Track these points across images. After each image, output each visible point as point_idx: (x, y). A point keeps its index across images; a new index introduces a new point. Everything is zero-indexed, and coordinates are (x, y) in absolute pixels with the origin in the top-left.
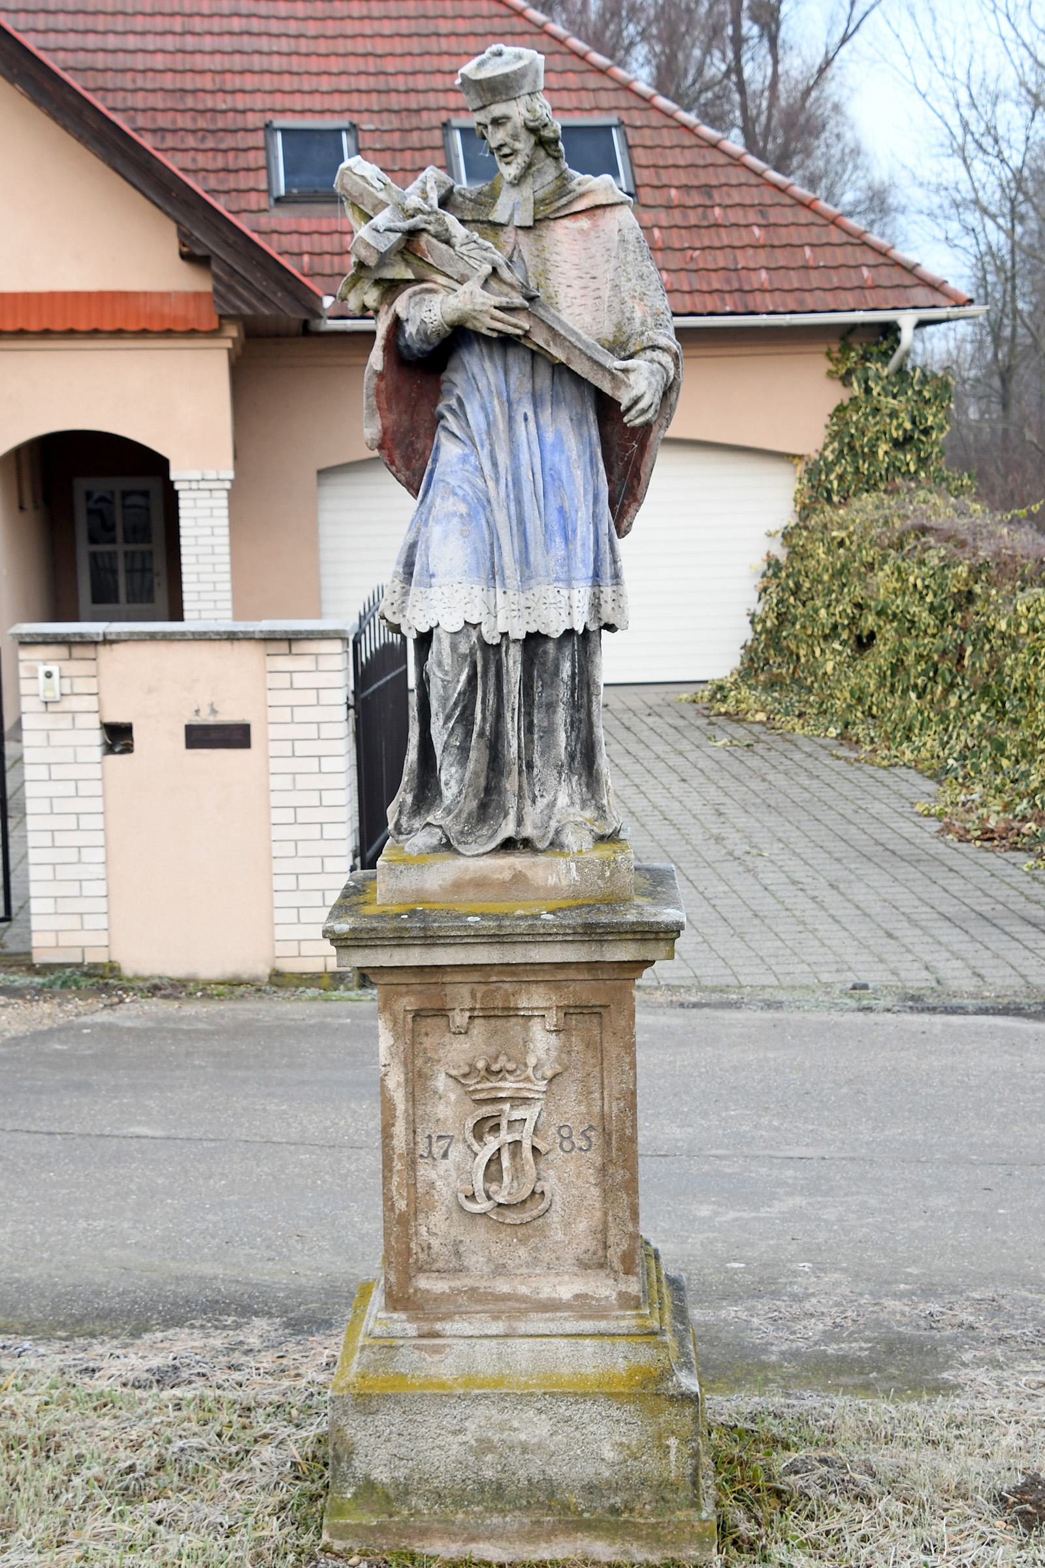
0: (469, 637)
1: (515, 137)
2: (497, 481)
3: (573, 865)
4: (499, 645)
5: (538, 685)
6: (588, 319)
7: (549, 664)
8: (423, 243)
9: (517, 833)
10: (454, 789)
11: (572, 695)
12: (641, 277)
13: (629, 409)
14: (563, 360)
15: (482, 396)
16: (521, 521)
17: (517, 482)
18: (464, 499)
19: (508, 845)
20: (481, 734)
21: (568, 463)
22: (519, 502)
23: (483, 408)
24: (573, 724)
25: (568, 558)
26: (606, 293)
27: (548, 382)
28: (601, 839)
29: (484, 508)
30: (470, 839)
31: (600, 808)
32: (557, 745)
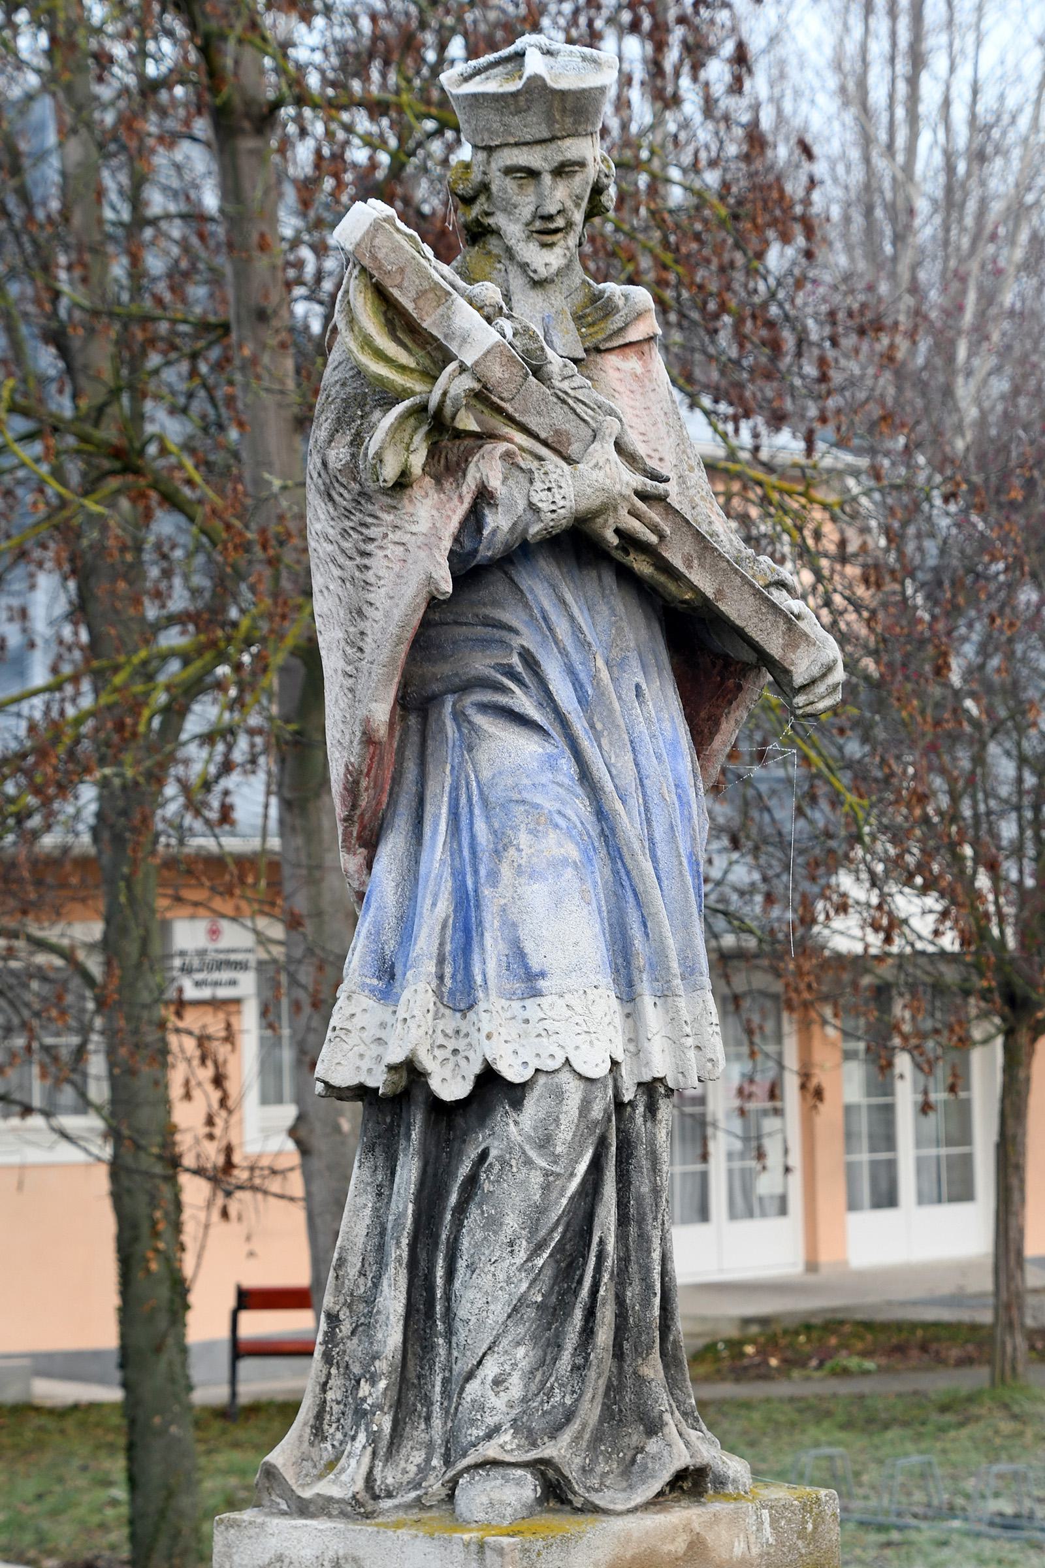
3: (765, 1513)
14: (709, 591)
15: (563, 652)
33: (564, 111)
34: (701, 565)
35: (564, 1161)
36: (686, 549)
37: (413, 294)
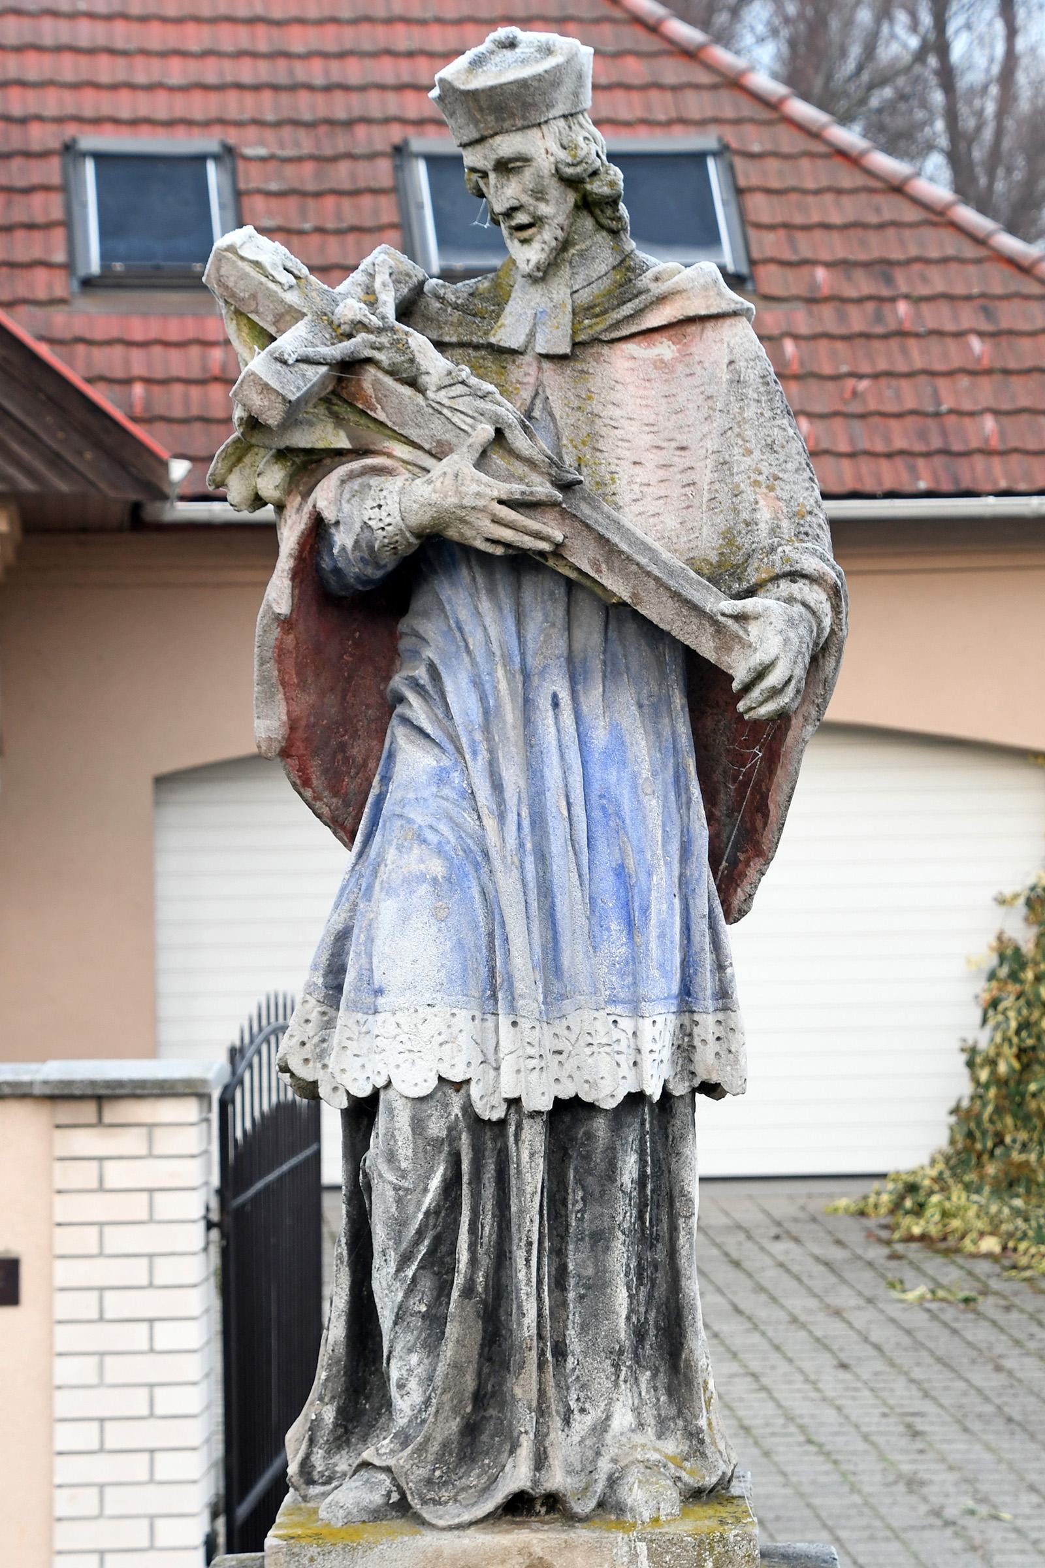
0: (446, 1106)
1: (539, 194)
2: (501, 817)
3: (642, 1547)
4: (502, 1123)
5: (575, 1196)
7: (598, 1157)
8: (367, 385)
9: (536, 1482)
10: (416, 1395)
11: (641, 1217)
12: (771, 447)
13: (747, 688)
14: (626, 596)
15: (474, 663)
16: (546, 890)
17: (538, 820)
18: (440, 851)
19: (518, 1507)
20: (468, 1291)
21: (634, 787)
22: (542, 857)
23: (477, 683)
24: (641, 1273)
25: (634, 960)
26: (705, 476)
27: (596, 638)
28: (696, 1495)
29: (477, 866)
30: (445, 1494)
31: (694, 1435)
32: (610, 1312)
33: (481, 110)
34: (611, 569)
35: (412, 1177)
36: (591, 554)
37: (270, 318)
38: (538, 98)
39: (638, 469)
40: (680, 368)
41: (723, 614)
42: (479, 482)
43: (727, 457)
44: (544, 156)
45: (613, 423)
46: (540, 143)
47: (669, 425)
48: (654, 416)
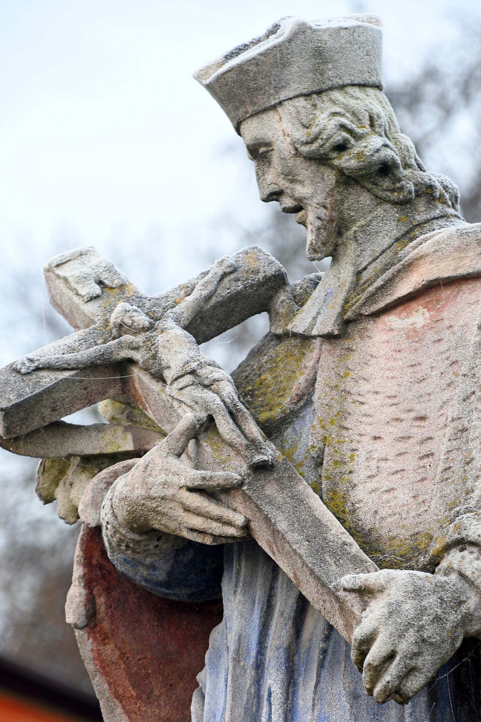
6: (403, 496)
26: (441, 446)
38: (261, 82)
39: (378, 444)
40: (430, 336)
41: (345, 590)
42: (167, 471)
43: (466, 424)
44: (281, 138)
45: (360, 399)
46: (277, 126)
47: (410, 395)
48: (396, 388)
